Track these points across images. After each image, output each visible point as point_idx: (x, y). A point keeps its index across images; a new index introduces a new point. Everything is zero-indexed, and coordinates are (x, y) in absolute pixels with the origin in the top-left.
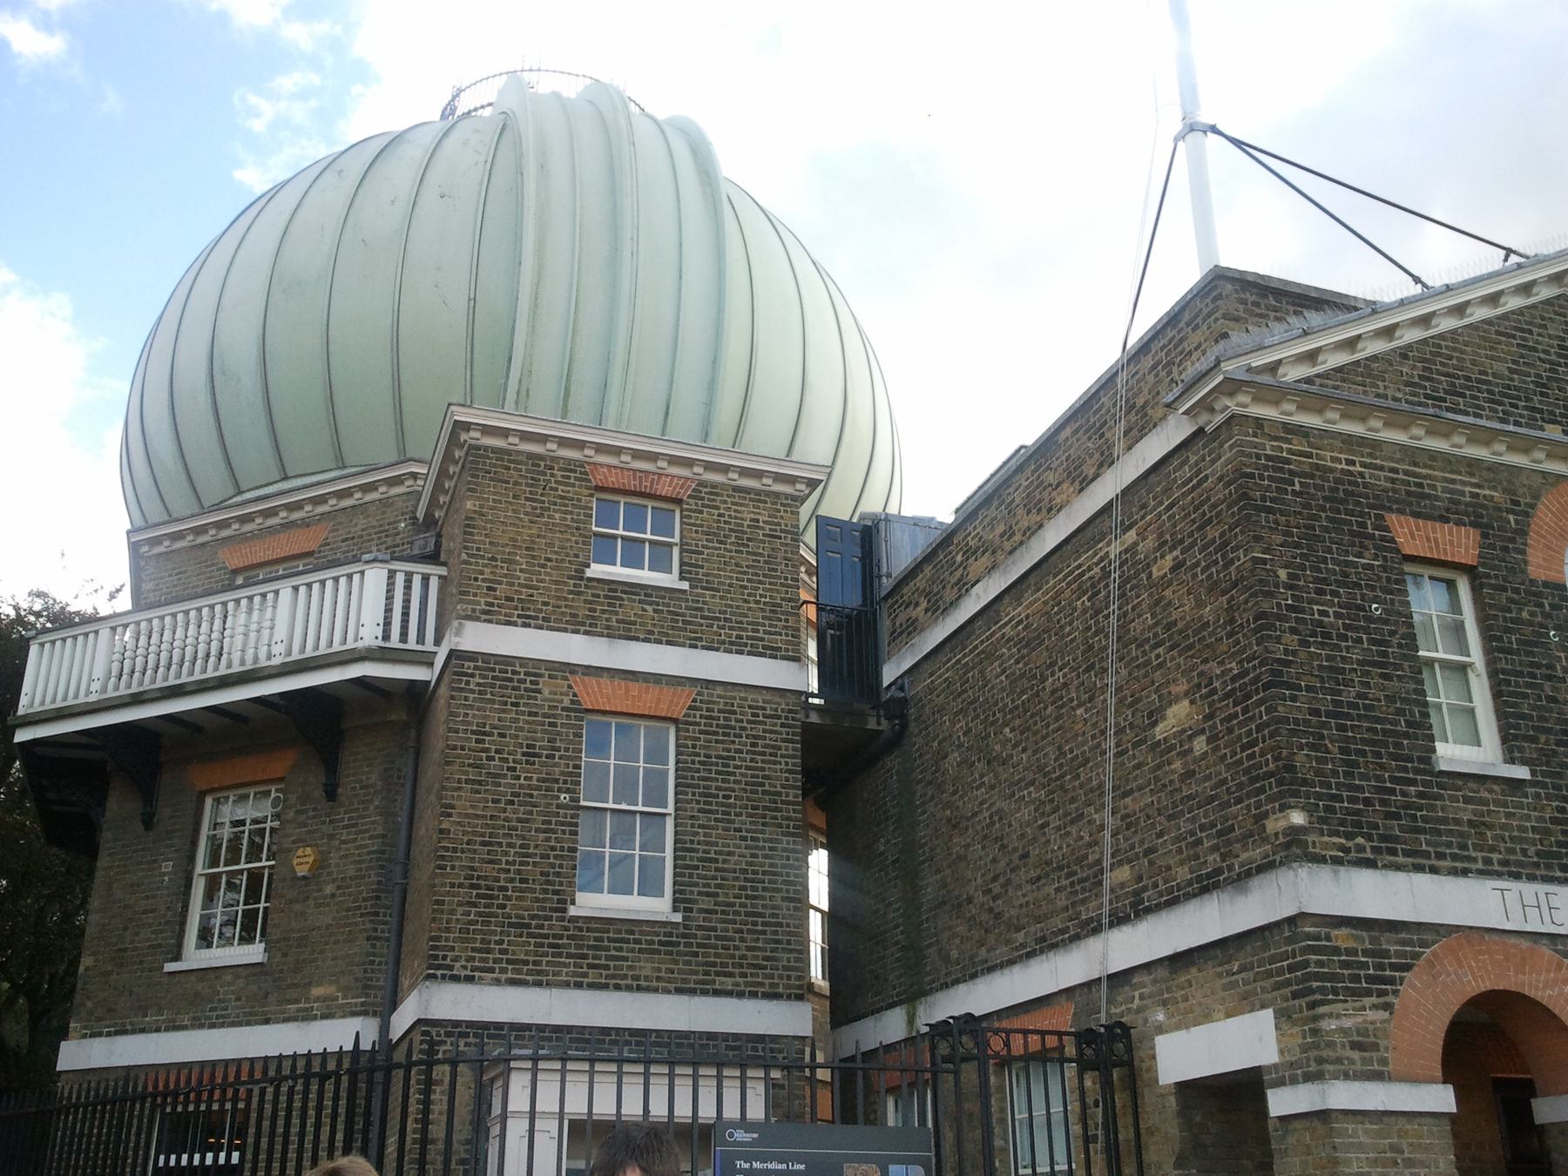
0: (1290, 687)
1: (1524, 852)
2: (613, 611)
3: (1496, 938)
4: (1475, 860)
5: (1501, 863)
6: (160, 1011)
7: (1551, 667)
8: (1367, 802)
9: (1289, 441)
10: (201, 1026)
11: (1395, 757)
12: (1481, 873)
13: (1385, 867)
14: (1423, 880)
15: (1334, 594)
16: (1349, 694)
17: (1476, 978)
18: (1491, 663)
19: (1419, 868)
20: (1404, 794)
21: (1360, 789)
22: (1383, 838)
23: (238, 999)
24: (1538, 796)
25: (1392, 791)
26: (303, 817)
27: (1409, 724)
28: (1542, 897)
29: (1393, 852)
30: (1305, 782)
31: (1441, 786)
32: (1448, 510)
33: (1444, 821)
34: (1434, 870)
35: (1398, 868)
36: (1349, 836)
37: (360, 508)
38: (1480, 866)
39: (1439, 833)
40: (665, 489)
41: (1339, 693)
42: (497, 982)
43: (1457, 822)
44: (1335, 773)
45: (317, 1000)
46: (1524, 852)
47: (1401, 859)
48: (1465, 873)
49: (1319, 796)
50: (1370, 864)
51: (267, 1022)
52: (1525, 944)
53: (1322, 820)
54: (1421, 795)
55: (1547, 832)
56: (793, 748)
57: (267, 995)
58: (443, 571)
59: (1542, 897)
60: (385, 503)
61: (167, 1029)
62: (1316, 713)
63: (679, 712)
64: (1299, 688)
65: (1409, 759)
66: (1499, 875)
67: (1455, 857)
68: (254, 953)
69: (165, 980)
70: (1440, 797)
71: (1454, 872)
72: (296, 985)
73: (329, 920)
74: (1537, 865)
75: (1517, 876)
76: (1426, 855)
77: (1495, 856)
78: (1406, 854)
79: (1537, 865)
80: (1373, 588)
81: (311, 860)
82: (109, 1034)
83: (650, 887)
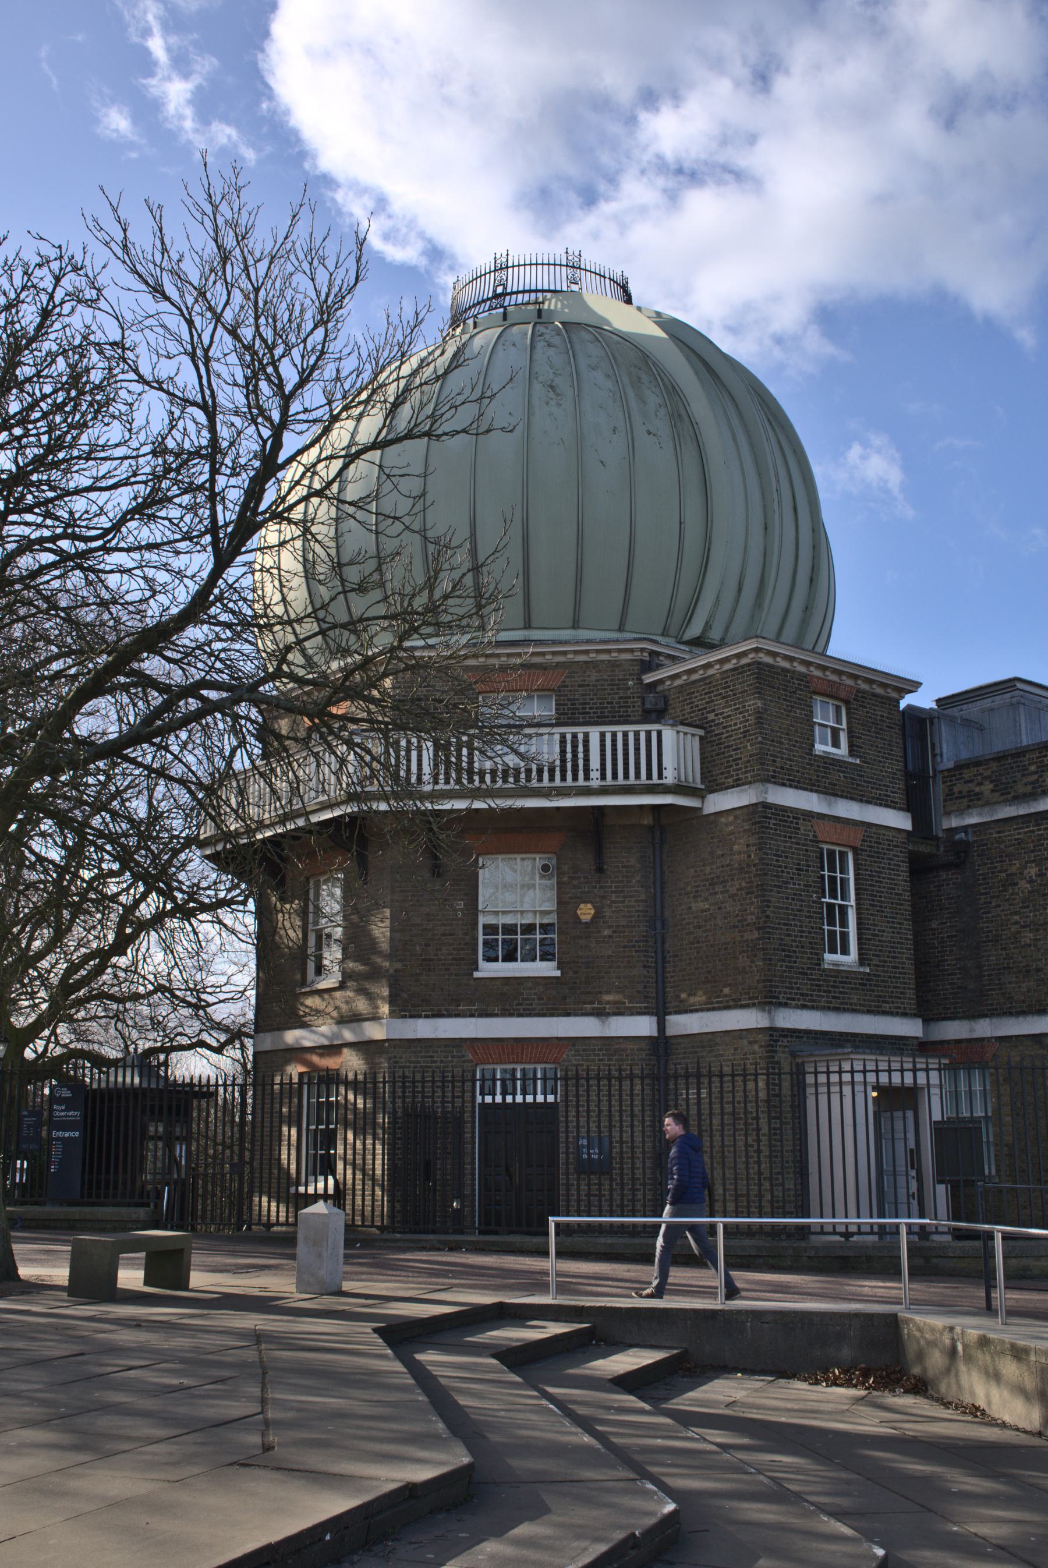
2: (823, 777)
6: (471, 1002)
10: (511, 1015)
23: (540, 999)
26: (575, 882)
37: (593, 665)
40: (843, 694)
42: (797, 1007)
45: (608, 1002)
51: (568, 1015)
56: (904, 867)
57: (565, 998)
58: (701, 732)
60: (614, 665)
61: (481, 1016)
63: (858, 844)
68: (547, 969)
69: (472, 982)
72: (589, 993)
73: (610, 953)
81: (593, 912)
82: (427, 1016)
83: (845, 951)
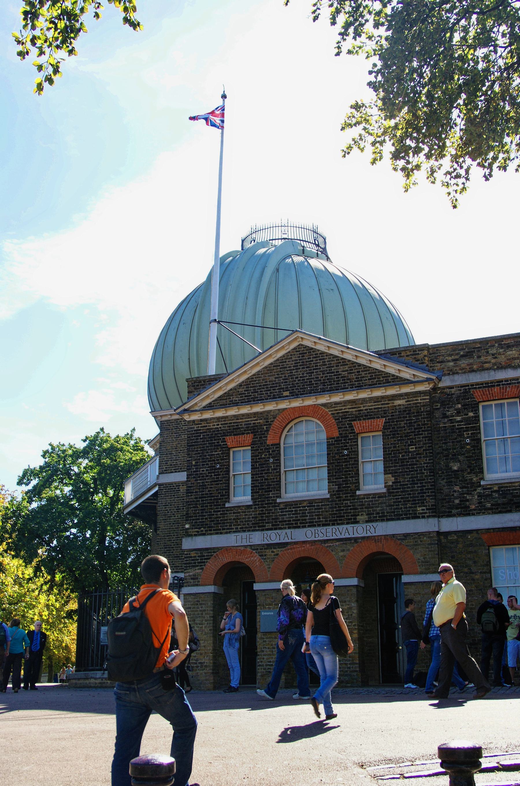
0: (191, 493)
1: (248, 524)
4: (233, 529)
5: (240, 528)
7: (268, 470)
8: (206, 519)
9: (201, 424)
11: (215, 505)
12: (234, 532)
13: (208, 534)
14: (215, 537)
15: (207, 464)
17: (226, 559)
19: (217, 533)
20: (216, 515)
21: (205, 516)
24: (256, 508)
25: (213, 515)
28: (248, 536)
29: (211, 530)
30: (191, 517)
31: (227, 511)
32: (245, 431)
33: (227, 520)
34: (221, 533)
35: (211, 534)
36: (199, 528)
38: (234, 530)
41: (203, 491)
43: (230, 519)
44: (198, 513)
46: (248, 524)
48: (230, 532)
49: (193, 520)
50: (204, 534)
52: (242, 548)
53: (193, 526)
54: (221, 514)
55: (256, 517)
59: (248, 536)
66: (239, 531)
70: (227, 514)
71: (226, 533)
74: (251, 527)
75: (244, 531)
76: (220, 530)
77: (239, 527)
78: (214, 530)
80: (218, 460)
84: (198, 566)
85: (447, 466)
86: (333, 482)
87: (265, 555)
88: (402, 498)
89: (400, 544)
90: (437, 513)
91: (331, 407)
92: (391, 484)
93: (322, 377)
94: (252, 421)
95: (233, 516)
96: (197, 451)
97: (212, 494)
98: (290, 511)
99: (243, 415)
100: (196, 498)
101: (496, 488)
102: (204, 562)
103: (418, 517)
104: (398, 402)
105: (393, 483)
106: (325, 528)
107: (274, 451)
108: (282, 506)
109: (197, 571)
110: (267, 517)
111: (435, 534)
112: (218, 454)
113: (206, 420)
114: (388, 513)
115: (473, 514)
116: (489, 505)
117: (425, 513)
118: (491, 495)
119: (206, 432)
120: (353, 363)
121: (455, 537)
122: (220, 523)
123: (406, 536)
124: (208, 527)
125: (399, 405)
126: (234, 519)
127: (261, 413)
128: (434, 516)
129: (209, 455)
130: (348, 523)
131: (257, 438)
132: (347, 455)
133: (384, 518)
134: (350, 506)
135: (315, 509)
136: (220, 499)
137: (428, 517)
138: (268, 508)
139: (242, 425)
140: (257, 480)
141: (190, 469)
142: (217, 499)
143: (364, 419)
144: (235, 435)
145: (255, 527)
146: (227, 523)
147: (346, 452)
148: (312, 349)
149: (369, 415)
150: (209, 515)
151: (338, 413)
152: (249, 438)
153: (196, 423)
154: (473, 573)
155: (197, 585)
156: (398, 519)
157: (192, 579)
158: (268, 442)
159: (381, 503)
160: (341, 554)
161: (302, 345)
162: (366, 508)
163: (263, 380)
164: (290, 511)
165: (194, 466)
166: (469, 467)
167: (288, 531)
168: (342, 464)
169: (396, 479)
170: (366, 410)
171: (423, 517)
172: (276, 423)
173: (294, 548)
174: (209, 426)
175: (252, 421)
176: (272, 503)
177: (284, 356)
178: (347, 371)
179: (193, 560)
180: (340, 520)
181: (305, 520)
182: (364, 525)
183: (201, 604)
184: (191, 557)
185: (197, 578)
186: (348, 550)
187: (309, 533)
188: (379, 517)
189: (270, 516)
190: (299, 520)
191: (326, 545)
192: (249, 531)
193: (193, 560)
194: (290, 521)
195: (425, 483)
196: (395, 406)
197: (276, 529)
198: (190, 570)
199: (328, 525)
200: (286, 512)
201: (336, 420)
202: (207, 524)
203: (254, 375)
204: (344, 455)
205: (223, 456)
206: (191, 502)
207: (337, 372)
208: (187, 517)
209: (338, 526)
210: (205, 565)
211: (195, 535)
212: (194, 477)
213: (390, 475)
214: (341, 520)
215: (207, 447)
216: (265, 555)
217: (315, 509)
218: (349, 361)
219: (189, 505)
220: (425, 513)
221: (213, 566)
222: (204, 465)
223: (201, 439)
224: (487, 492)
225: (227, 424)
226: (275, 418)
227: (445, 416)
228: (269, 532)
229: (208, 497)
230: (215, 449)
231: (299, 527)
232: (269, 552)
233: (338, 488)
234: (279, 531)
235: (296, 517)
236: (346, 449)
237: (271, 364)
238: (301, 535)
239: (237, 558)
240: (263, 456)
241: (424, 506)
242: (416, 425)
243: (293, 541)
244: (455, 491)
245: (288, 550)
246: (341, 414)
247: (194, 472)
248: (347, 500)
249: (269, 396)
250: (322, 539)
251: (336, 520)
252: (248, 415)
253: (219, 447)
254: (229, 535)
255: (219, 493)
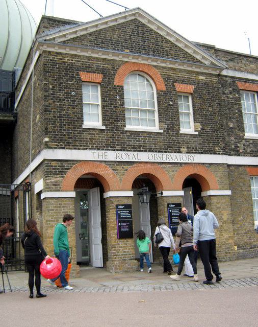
0: (48, 111)
3: (92, 162)
4: (89, 146)
5: (96, 147)
8: (65, 135)
11: (72, 125)
12: (90, 149)
16: (64, 112)
18: (102, 103)
19: (75, 149)
20: (74, 133)
21: (63, 133)
22: (67, 143)
25: (71, 133)
27: (77, 118)
28: (104, 154)
29: (69, 146)
33: (83, 138)
34: (79, 149)
38: (90, 147)
39: (81, 141)
41: (61, 112)
43: (86, 139)
44: (57, 130)
47: (71, 147)
48: (86, 149)
52: (98, 163)
54: (78, 133)
59: (104, 154)
62: (55, 117)
64: (51, 112)
65: (76, 126)
66: (95, 149)
67: (85, 146)
71: (84, 149)
74: (105, 147)
75: (99, 149)
78: (72, 146)
79: (105, 147)
84: (58, 174)
85: (227, 124)
86: (164, 122)
87: (117, 170)
88: (207, 140)
89: (208, 170)
90: (227, 151)
91: (160, 69)
92: (200, 129)
93: (152, 47)
94: (101, 64)
95: (89, 136)
96: (53, 77)
97: (69, 115)
98: (134, 138)
99: (94, 58)
100: (53, 117)
101: (251, 142)
102: (65, 172)
103: (217, 154)
104: (201, 77)
105: (201, 129)
106: (162, 154)
107: (121, 91)
108: (128, 134)
109: (59, 179)
110: (117, 140)
111: (226, 166)
112: (73, 84)
113: (61, 54)
114: (199, 148)
115: (242, 156)
116: (249, 151)
117: (220, 151)
118: (249, 145)
119: (61, 64)
120: (172, 43)
121: (234, 169)
122: (78, 141)
123: (211, 164)
124: (67, 143)
125: (202, 79)
126: (89, 138)
127: (109, 60)
128: (225, 154)
129: (64, 83)
130: (175, 152)
131: (106, 78)
132: (172, 105)
133: (196, 151)
134: (176, 141)
135: (153, 139)
136: (77, 121)
137: (222, 154)
138: (115, 133)
139: (93, 65)
140: (108, 111)
141: (47, 91)
142: (75, 121)
143: (182, 83)
144: (87, 72)
145: (108, 147)
146: (84, 141)
147: (171, 103)
148: (144, 25)
149: (184, 82)
150: (67, 133)
151: (165, 75)
152: (98, 78)
153: (51, 54)
154: (243, 191)
155: (59, 191)
156: (205, 153)
157: (54, 185)
158: (115, 83)
159: (195, 142)
160: (172, 173)
161: (137, 20)
162: (186, 143)
163: (109, 36)
164: (134, 138)
165: (52, 89)
166: (238, 127)
167: (135, 153)
168: (168, 110)
169: (202, 127)
170: (182, 77)
171: (219, 154)
172: (121, 71)
173: (139, 166)
174: (64, 59)
175: (101, 64)
176: (120, 130)
177: (124, 23)
178: (168, 47)
179: (54, 169)
180: (170, 149)
181: (146, 146)
182: (187, 155)
183: (63, 207)
184: (52, 166)
185: (59, 185)
186: (176, 171)
187: (150, 157)
188: (194, 150)
189: (119, 140)
190: (141, 146)
191: (162, 166)
192: (103, 149)
193: (54, 169)
194: (135, 146)
195: (219, 132)
196: (199, 79)
197: (124, 150)
198: (51, 178)
199: (162, 152)
200: (131, 138)
201: (164, 79)
202: (66, 140)
203: (101, 30)
204: (169, 105)
205: (78, 87)
206: (50, 119)
207: (162, 46)
208: (46, 132)
209: (170, 154)
210: (65, 174)
211: (55, 148)
212: (52, 99)
213: (199, 124)
214: (170, 149)
215: (63, 76)
216: (117, 170)
217: (153, 139)
218: (170, 41)
219: (48, 121)
220: (220, 151)
221: (72, 176)
222: (61, 90)
223: (57, 68)
224: (248, 143)
225: (80, 61)
226: (119, 66)
227: (224, 93)
228: (121, 153)
229: (65, 117)
230: (70, 79)
231: (142, 151)
232: (119, 167)
233: (168, 127)
234: (128, 153)
235: (139, 143)
236: (171, 101)
237: (115, 26)
238: (144, 157)
239: (94, 171)
240: (112, 93)
241: (219, 147)
242: (212, 94)
243: (139, 161)
244: (232, 140)
245: (135, 167)
246: (167, 76)
247: (52, 94)
248: (174, 136)
249: (114, 49)
250: (159, 161)
251: (167, 149)
252: (98, 59)
253: (74, 79)
254: (86, 151)
255: (75, 116)
